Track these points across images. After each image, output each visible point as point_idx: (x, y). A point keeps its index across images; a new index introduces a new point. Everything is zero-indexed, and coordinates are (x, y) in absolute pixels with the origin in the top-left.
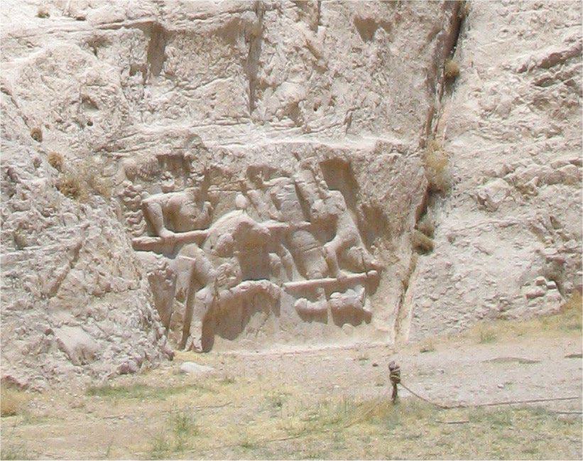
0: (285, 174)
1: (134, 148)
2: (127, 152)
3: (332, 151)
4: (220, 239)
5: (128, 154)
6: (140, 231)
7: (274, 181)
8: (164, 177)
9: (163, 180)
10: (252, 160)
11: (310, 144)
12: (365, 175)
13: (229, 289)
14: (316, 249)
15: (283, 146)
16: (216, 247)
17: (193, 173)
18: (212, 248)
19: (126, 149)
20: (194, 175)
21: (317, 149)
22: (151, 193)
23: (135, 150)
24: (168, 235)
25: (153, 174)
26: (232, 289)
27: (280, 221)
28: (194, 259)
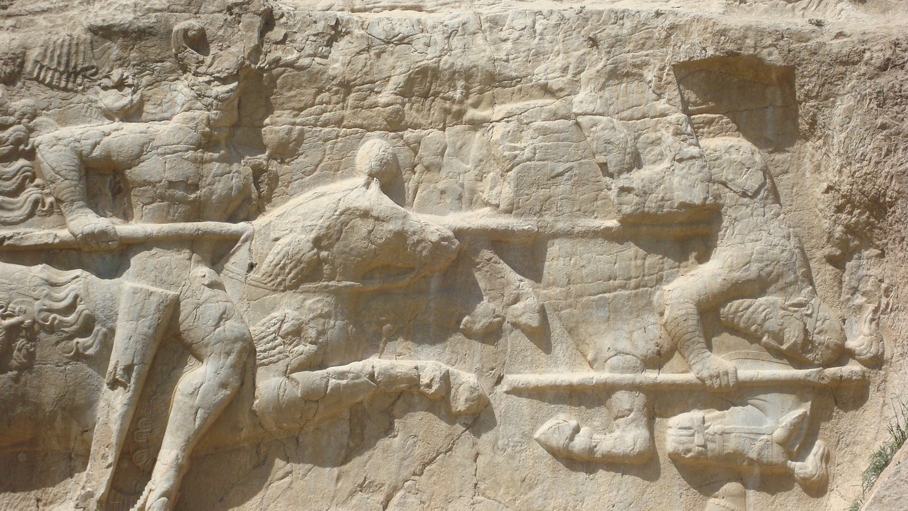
0: (546, 90)
1: (30, 7)
2: (9, 16)
3: (723, 32)
4: (278, 246)
5: (10, 22)
6: (17, 213)
7: (500, 110)
8: (105, 82)
9: (105, 88)
10: (432, 53)
11: (658, 14)
12: (852, 103)
13: (286, 373)
14: (626, 292)
15: (563, 18)
16: (264, 267)
17: (196, 74)
18: (251, 267)
19: (10, 10)
20: (201, 79)
21: (673, 27)
22: (63, 121)
23: (35, 13)
24: (87, 229)
25: (72, 73)
26: (294, 375)
27: (509, 211)
28: (172, 293)
